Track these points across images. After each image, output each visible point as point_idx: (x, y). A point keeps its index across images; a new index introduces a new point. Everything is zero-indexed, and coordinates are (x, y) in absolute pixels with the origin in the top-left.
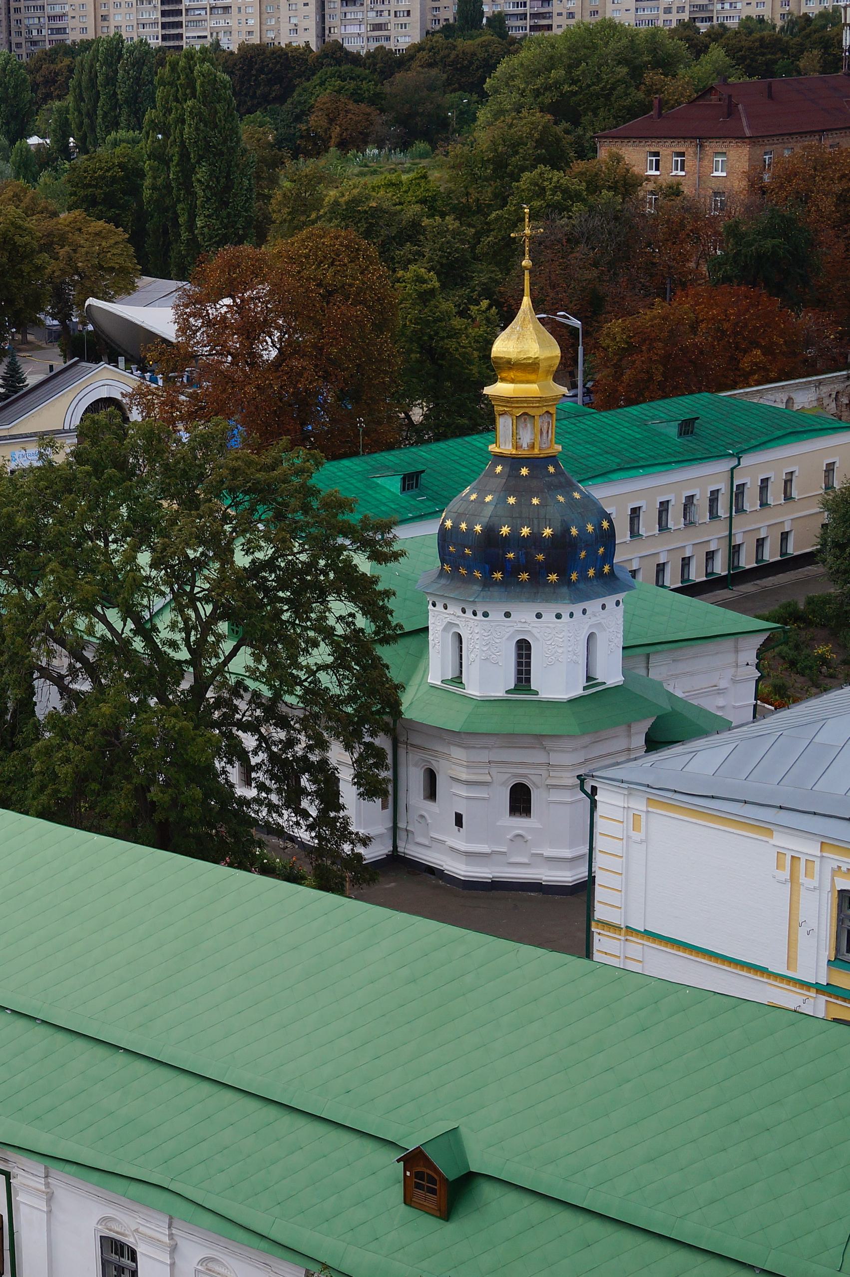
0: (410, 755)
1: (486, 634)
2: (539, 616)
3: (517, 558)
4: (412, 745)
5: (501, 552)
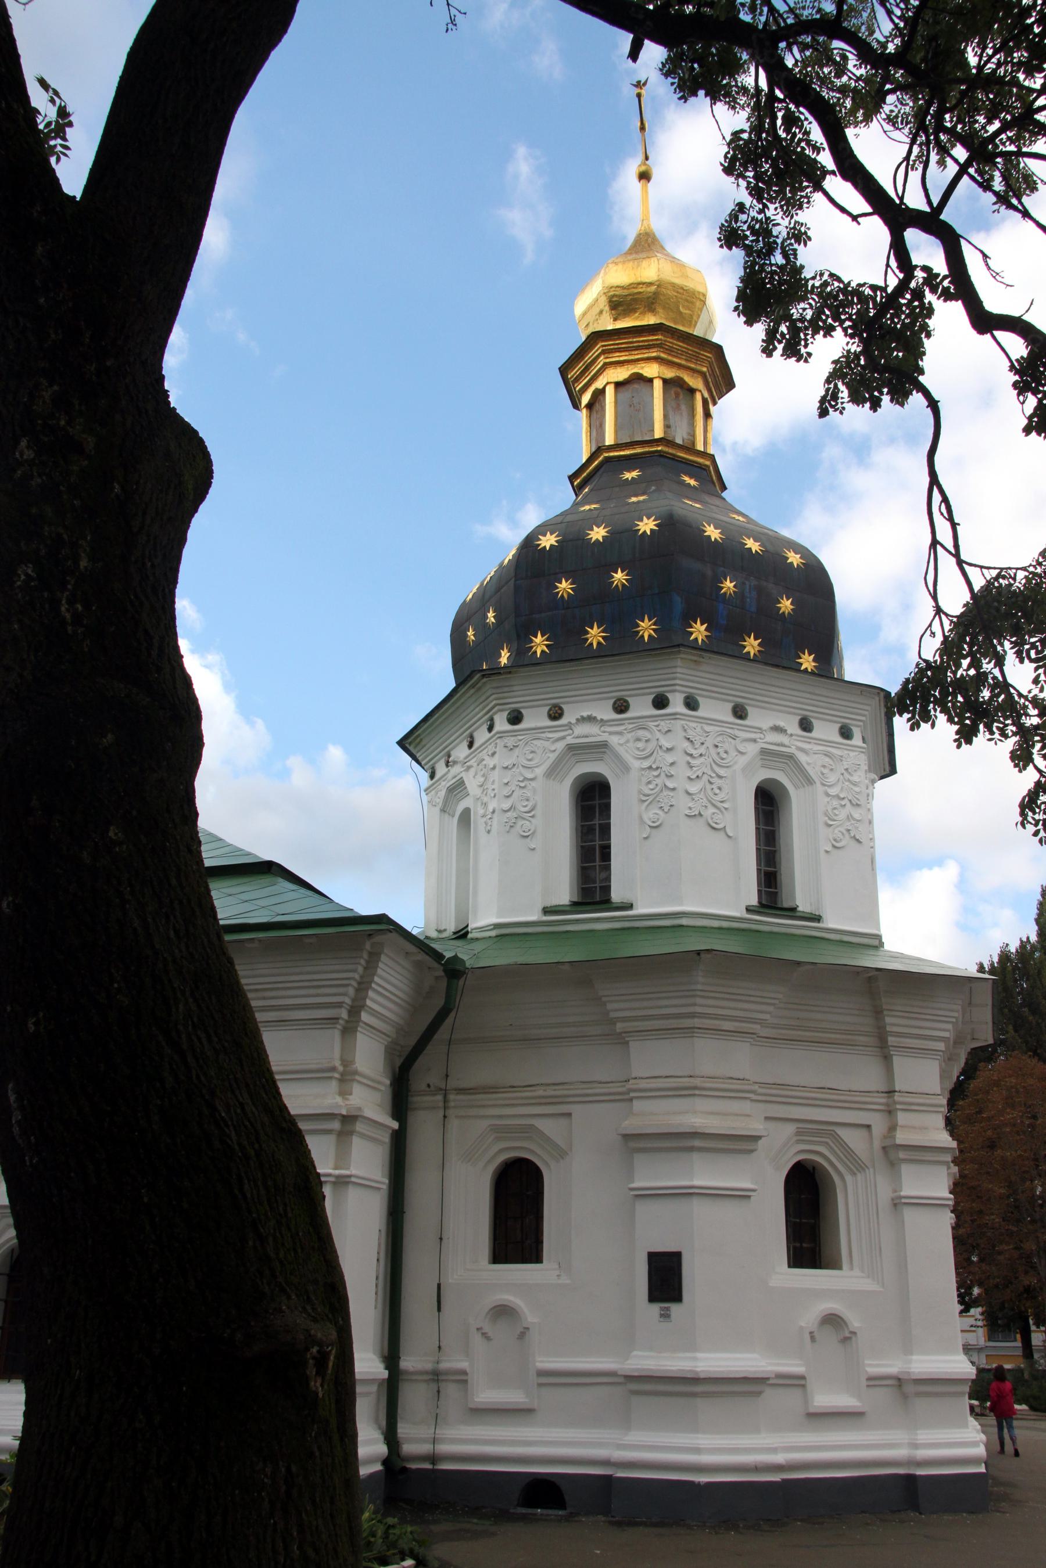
0: (454, 1124)
1: (693, 752)
2: (806, 725)
3: (740, 594)
4: (461, 1091)
5: (709, 573)
